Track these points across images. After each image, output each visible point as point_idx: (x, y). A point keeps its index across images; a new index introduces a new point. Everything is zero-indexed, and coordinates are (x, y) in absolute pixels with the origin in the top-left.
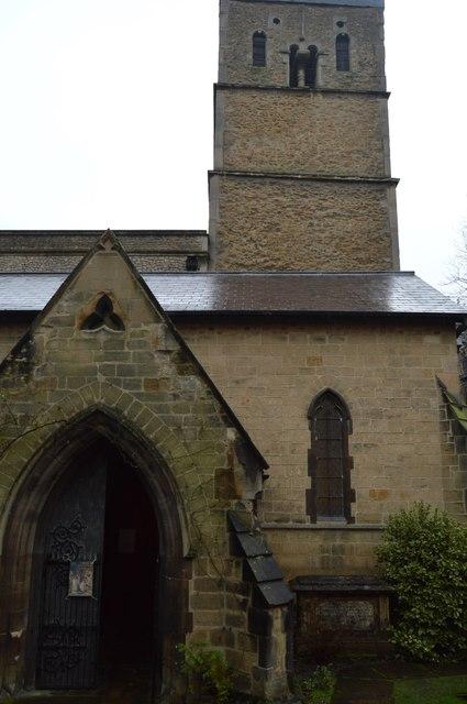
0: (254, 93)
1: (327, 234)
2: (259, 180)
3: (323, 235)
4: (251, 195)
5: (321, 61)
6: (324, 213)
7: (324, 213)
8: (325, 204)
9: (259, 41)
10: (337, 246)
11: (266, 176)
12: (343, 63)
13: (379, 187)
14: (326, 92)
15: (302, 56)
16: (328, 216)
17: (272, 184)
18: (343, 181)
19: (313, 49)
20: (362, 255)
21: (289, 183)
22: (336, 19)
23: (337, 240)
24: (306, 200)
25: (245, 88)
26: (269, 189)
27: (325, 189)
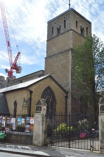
0: (51, 40)
4: (50, 60)
5: (61, 28)
12: (65, 27)
13: (68, 51)
14: (62, 34)
18: (62, 52)
19: (60, 26)
20: (65, 67)
21: (55, 56)
25: (50, 39)
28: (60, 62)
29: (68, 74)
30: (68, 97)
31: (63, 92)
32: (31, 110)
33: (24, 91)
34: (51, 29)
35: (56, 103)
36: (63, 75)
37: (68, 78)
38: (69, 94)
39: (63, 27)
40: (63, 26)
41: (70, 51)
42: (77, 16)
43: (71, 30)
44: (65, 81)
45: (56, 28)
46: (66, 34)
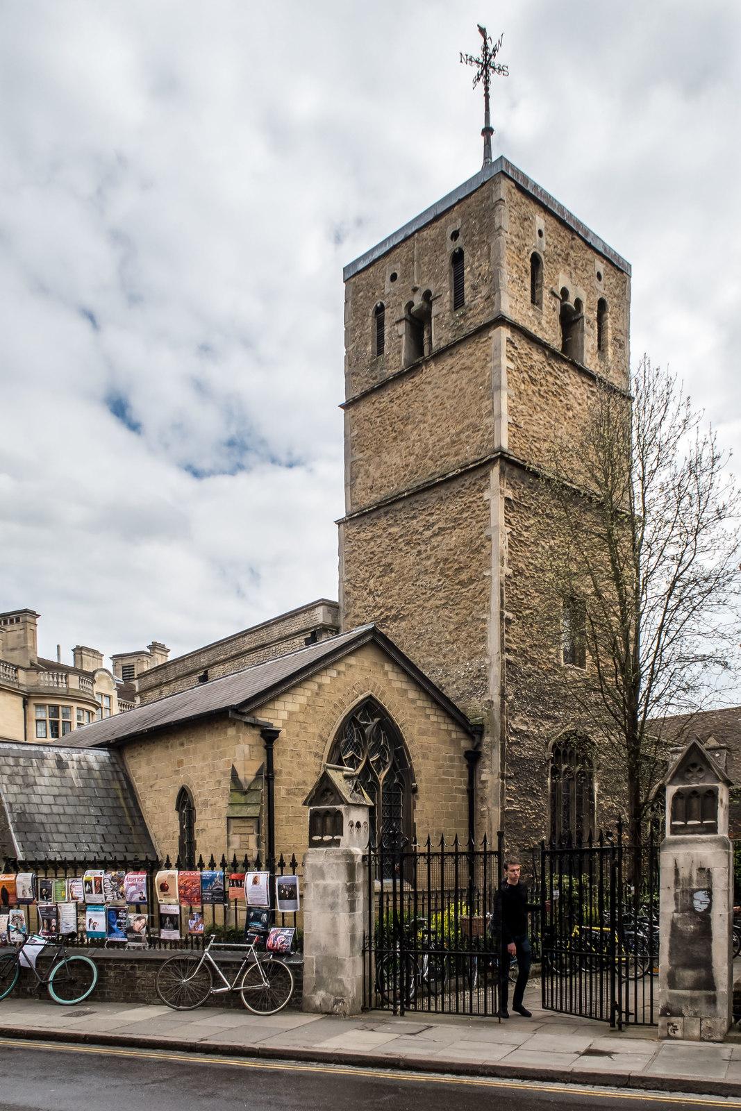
5: (435, 310)
16: (435, 535)
19: (427, 296)
23: (441, 565)
39: (448, 306)
40: (448, 296)
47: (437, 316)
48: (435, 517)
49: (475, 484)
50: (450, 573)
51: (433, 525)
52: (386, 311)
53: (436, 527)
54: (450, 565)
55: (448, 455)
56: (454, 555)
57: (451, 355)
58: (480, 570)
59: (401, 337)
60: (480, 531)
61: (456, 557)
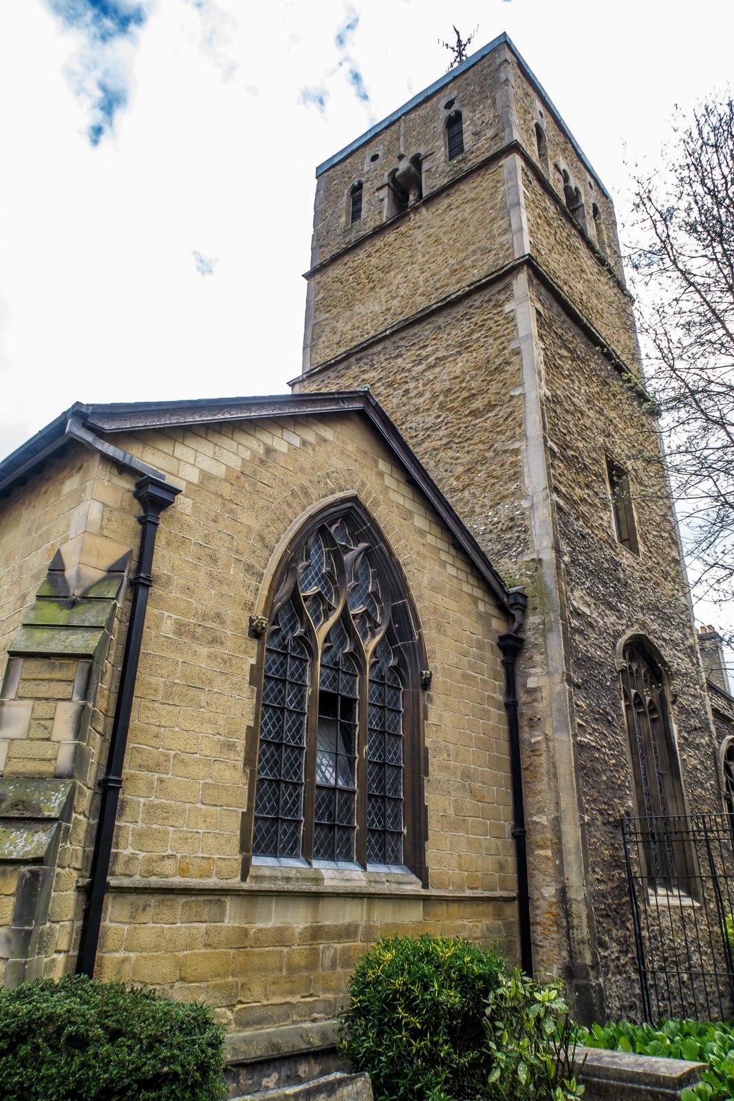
0: (346, 259)
1: (428, 395)
2: (343, 365)
3: (422, 400)
6: (423, 367)
7: (423, 367)
8: (424, 353)
9: (357, 189)
10: (442, 406)
11: (348, 355)
13: (501, 285)
15: (406, 173)
16: (430, 367)
17: (358, 360)
19: (417, 161)
20: (478, 404)
22: (443, 102)
23: (441, 398)
24: (400, 360)
25: (335, 259)
26: (355, 369)
27: (425, 330)
28: (429, 375)
29: (516, 452)
30: (522, 641)
31: (478, 593)
32: (138, 718)
33: (71, 484)
34: (345, 201)
35: (426, 684)
36: (460, 469)
37: (516, 476)
38: (533, 620)
39: (443, 158)
40: (442, 152)
41: (521, 282)
42: (539, 106)
43: (514, 147)
44: (478, 510)
45: (386, 180)
46: (465, 187)
47: (427, 171)
48: (429, 349)
49: (489, 300)
50: (455, 405)
51: (427, 357)
52: (364, 185)
53: (431, 360)
54: (455, 396)
55: (447, 285)
56: (461, 382)
57: (448, 195)
58: (503, 391)
59: (382, 200)
60: (501, 347)
61: (464, 385)
